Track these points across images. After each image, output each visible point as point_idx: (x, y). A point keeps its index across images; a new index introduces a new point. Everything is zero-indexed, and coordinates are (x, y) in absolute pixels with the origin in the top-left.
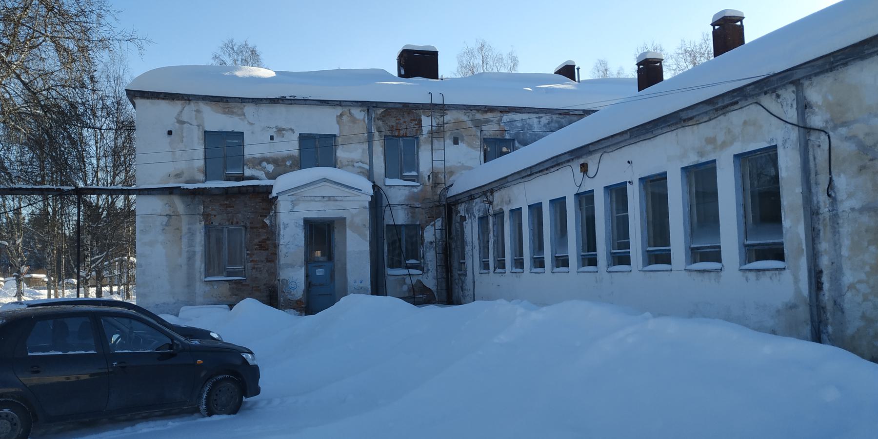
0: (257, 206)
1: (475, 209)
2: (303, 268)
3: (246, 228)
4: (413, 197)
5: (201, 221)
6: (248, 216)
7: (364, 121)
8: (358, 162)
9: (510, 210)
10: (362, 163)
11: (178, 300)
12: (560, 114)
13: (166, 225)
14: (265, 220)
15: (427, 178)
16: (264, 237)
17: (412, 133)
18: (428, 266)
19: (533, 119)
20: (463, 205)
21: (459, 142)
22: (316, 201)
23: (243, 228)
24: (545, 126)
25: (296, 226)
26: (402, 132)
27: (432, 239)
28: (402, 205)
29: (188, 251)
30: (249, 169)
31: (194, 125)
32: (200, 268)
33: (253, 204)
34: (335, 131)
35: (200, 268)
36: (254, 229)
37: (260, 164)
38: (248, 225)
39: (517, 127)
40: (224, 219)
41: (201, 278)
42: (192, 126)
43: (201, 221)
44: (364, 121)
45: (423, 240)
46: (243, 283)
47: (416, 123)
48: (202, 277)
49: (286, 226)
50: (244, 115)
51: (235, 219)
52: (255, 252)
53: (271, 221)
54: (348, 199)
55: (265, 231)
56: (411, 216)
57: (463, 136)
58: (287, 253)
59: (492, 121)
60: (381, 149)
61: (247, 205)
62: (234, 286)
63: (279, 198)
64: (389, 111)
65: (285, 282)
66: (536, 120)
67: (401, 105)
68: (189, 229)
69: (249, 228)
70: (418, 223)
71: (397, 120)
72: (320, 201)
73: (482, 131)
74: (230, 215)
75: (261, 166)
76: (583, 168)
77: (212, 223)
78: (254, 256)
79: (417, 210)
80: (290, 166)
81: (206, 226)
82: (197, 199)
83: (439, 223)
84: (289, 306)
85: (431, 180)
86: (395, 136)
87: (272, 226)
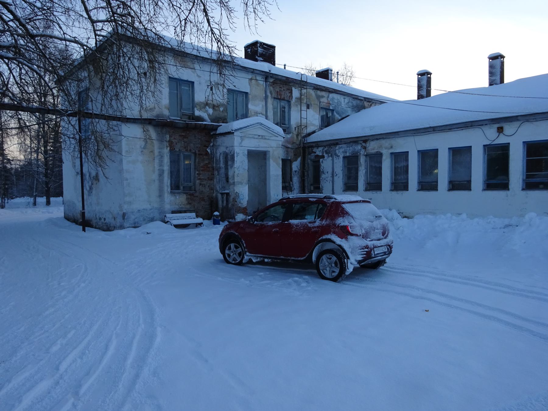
0: (202, 139)
2: (247, 185)
3: (195, 154)
4: (287, 141)
5: (167, 147)
7: (263, 86)
8: (260, 114)
9: (391, 153)
11: (153, 207)
12: (354, 98)
13: (144, 148)
14: (207, 150)
15: (294, 129)
16: (207, 162)
18: (294, 187)
20: (321, 149)
22: (254, 138)
23: (193, 155)
24: (346, 104)
26: (282, 97)
27: (297, 169)
29: (159, 170)
32: (168, 183)
33: (200, 137)
34: (248, 91)
35: (168, 183)
38: (197, 152)
39: (335, 103)
45: (291, 169)
46: (195, 195)
49: (238, 154)
51: (189, 147)
52: (201, 172)
53: (211, 150)
54: (272, 138)
55: (207, 157)
57: (311, 105)
58: (238, 174)
59: (324, 97)
61: (196, 138)
62: (189, 197)
63: (235, 134)
64: (276, 81)
65: (237, 195)
66: (343, 100)
67: (285, 78)
68: (160, 152)
71: (281, 88)
72: (257, 138)
73: (320, 102)
74: (186, 144)
76: (501, 130)
78: (201, 176)
79: (289, 150)
80: (222, 111)
81: (170, 150)
82: (165, 130)
83: (299, 159)
84: (240, 212)
85: (296, 130)
87: (211, 154)
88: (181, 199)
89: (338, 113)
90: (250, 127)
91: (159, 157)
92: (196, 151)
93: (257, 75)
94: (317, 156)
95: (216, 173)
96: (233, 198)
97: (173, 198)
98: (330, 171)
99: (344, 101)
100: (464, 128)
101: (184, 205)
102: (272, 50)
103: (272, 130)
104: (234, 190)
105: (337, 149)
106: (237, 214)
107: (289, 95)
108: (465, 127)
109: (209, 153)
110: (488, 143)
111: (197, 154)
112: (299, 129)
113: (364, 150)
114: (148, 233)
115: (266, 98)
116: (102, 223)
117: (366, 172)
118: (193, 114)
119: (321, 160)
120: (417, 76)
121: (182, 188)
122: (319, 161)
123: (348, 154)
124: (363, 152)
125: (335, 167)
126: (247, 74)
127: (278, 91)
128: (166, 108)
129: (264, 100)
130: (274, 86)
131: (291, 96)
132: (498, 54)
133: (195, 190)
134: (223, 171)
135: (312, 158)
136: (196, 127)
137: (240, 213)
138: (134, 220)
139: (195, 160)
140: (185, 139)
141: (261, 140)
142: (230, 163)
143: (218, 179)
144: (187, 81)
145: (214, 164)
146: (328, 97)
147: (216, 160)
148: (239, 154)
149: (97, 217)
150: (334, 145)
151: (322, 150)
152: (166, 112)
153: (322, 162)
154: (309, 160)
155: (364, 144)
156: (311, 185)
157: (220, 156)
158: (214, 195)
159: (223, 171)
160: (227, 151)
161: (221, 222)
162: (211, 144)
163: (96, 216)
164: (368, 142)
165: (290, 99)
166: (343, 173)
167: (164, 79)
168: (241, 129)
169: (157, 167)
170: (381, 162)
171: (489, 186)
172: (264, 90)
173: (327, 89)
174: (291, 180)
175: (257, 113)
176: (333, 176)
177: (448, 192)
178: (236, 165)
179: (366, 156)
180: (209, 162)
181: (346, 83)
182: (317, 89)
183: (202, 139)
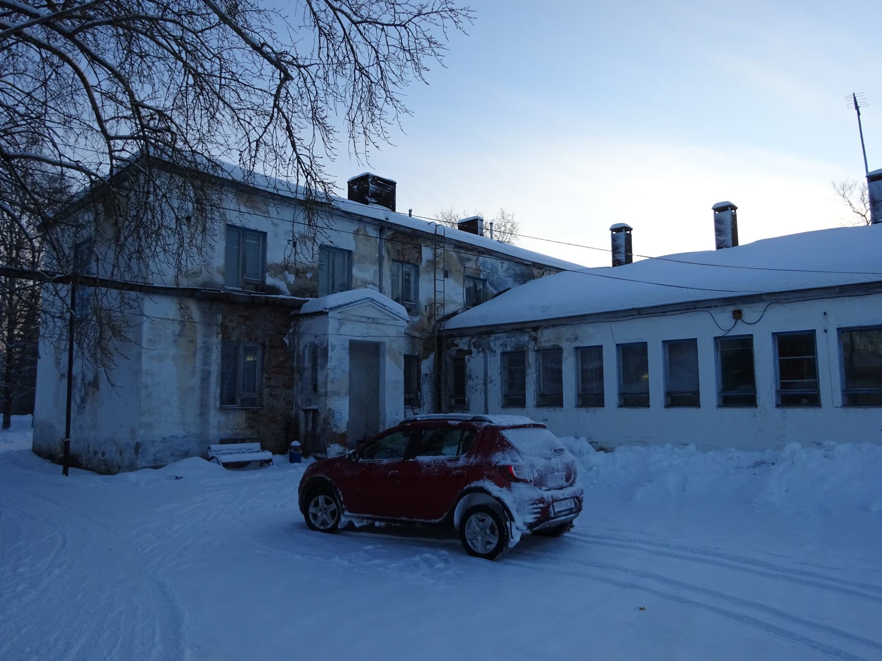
1: (495, 344)
4: (413, 327)
5: (218, 334)
8: (370, 284)
9: (575, 348)
12: (516, 262)
13: (179, 335)
14: (284, 339)
15: (424, 308)
16: (282, 359)
19: (498, 263)
20: (466, 340)
24: (505, 271)
25: (343, 348)
26: (406, 258)
29: (202, 371)
32: (215, 393)
33: (272, 319)
34: (352, 247)
35: (215, 393)
37: (282, 273)
41: (216, 405)
43: (218, 334)
48: (217, 403)
50: (268, 212)
51: (254, 335)
53: (290, 339)
57: (451, 271)
58: (333, 379)
59: (472, 259)
63: (330, 314)
65: (331, 413)
66: (500, 265)
67: (410, 231)
68: (205, 342)
69: (268, 346)
70: (416, 354)
72: (365, 322)
73: (465, 268)
76: (739, 315)
77: (230, 337)
79: (416, 340)
80: (311, 279)
81: (223, 339)
83: (432, 356)
87: (290, 346)
88: (237, 420)
89: (492, 285)
90: (354, 304)
92: (265, 341)
93: (366, 224)
94: (461, 350)
95: (297, 376)
96: (324, 419)
97: (223, 418)
98: (481, 375)
99: (502, 267)
100: (685, 311)
101: (241, 429)
102: (392, 188)
103: (389, 310)
104: (326, 406)
105: (492, 341)
106: (329, 444)
108: (686, 310)
110: (720, 333)
111: (268, 346)
112: (431, 308)
113: (533, 343)
114: (177, 478)
115: (380, 259)
116: (99, 460)
117: (538, 378)
118: (264, 282)
119: (467, 357)
120: (610, 232)
121: (239, 401)
122: (464, 359)
123: (509, 349)
124: (532, 345)
125: (488, 368)
126: (352, 222)
127: (399, 250)
129: (377, 263)
131: (420, 258)
132: (728, 204)
133: (261, 405)
134: (308, 374)
135: (453, 354)
136: (267, 303)
137: (335, 443)
138: (155, 455)
139: (263, 355)
140: (248, 322)
141: (372, 324)
142: (320, 361)
143: (300, 386)
144: (255, 231)
145: (293, 361)
146: (477, 260)
147: (297, 356)
148: (335, 346)
149: (91, 449)
150: (487, 334)
151: (469, 341)
152: (219, 279)
153: (469, 360)
154: (448, 358)
155: (533, 333)
156: (451, 397)
157: (304, 350)
158: (293, 412)
159: (308, 374)
160: (316, 342)
161: (303, 459)
162: (291, 331)
163: (88, 447)
164: (540, 330)
165: (419, 262)
166: (501, 378)
167: (219, 228)
168: (340, 306)
169: (198, 365)
170: (560, 362)
171: (727, 400)
172: (377, 247)
173: (476, 248)
174: (419, 388)
176: (485, 384)
177: (665, 409)
178: (330, 364)
179: (537, 351)
180: (286, 360)
181: (505, 238)
182: (461, 248)
183: (277, 322)
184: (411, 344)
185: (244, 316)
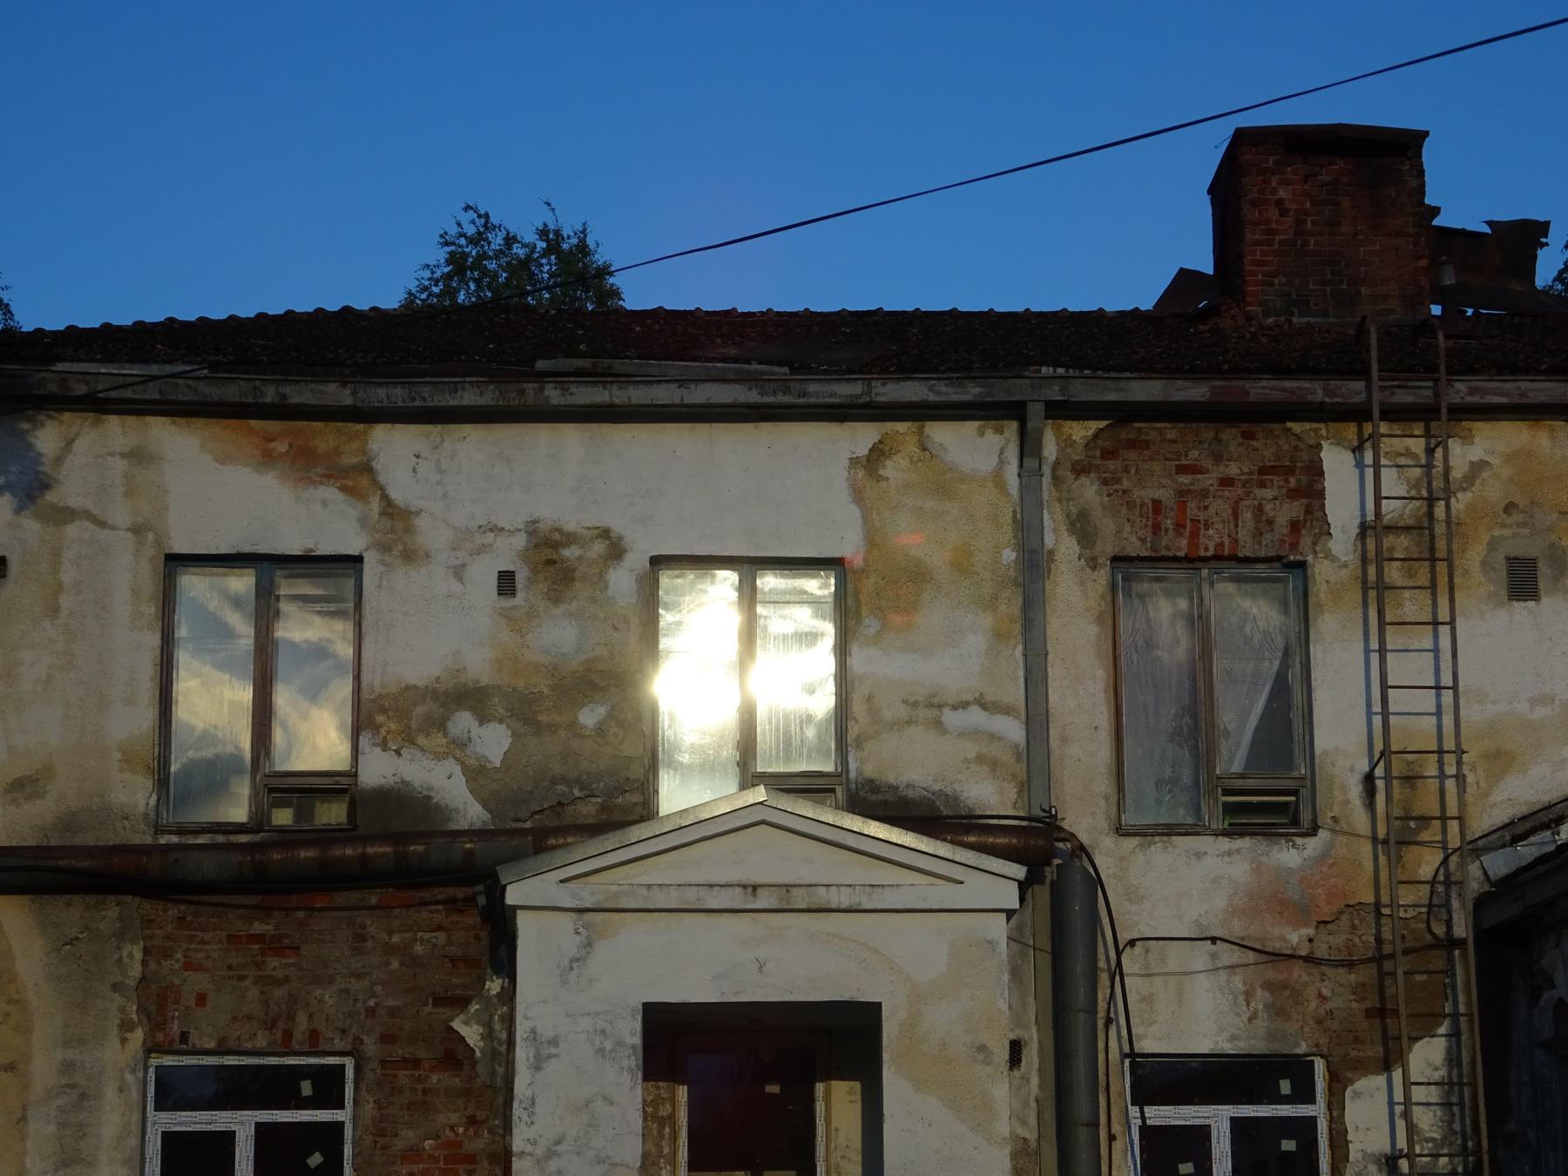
5: (126, 1026)
6: (371, 1003)
8: (964, 705)
10: (984, 706)
14: (457, 1025)
15: (1355, 792)
17: (1267, 538)
21: (1542, 585)
25: (601, 1051)
28: (1214, 940)
30: (385, 747)
31: (113, 528)
33: (396, 939)
36: (401, 1073)
37: (442, 726)
38: (370, 1046)
40: (249, 1018)
42: (104, 534)
43: (126, 1026)
44: (998, 477)
47: (1293, 482)
50: (367, 469)
53: (488, 1025)
55: (457, 1080)
56: (1266, 1006)
60: (1093, 630)
61: (370, 944)
68: (68, 1067)
69: (374, 1064)
71: (1182, 470)
74: (278, 993)
75: (445, 734)
82: (113, 913)
85: (1380, 799)
86: (1176, 559)
91: (59, 1102)
92: (358, 1041)
107: (1285, 513)
109: (473, 1050)
127: (1157, 506)
128: (128, 760)
130: (1112, 465)
140: (273, 962)
162: (494, 986)
165: (1306, 541)
172: (1008, 519)
175: (930, 705)
183: (418, 948)
184: (1262, 996)
185: (259, 938)
